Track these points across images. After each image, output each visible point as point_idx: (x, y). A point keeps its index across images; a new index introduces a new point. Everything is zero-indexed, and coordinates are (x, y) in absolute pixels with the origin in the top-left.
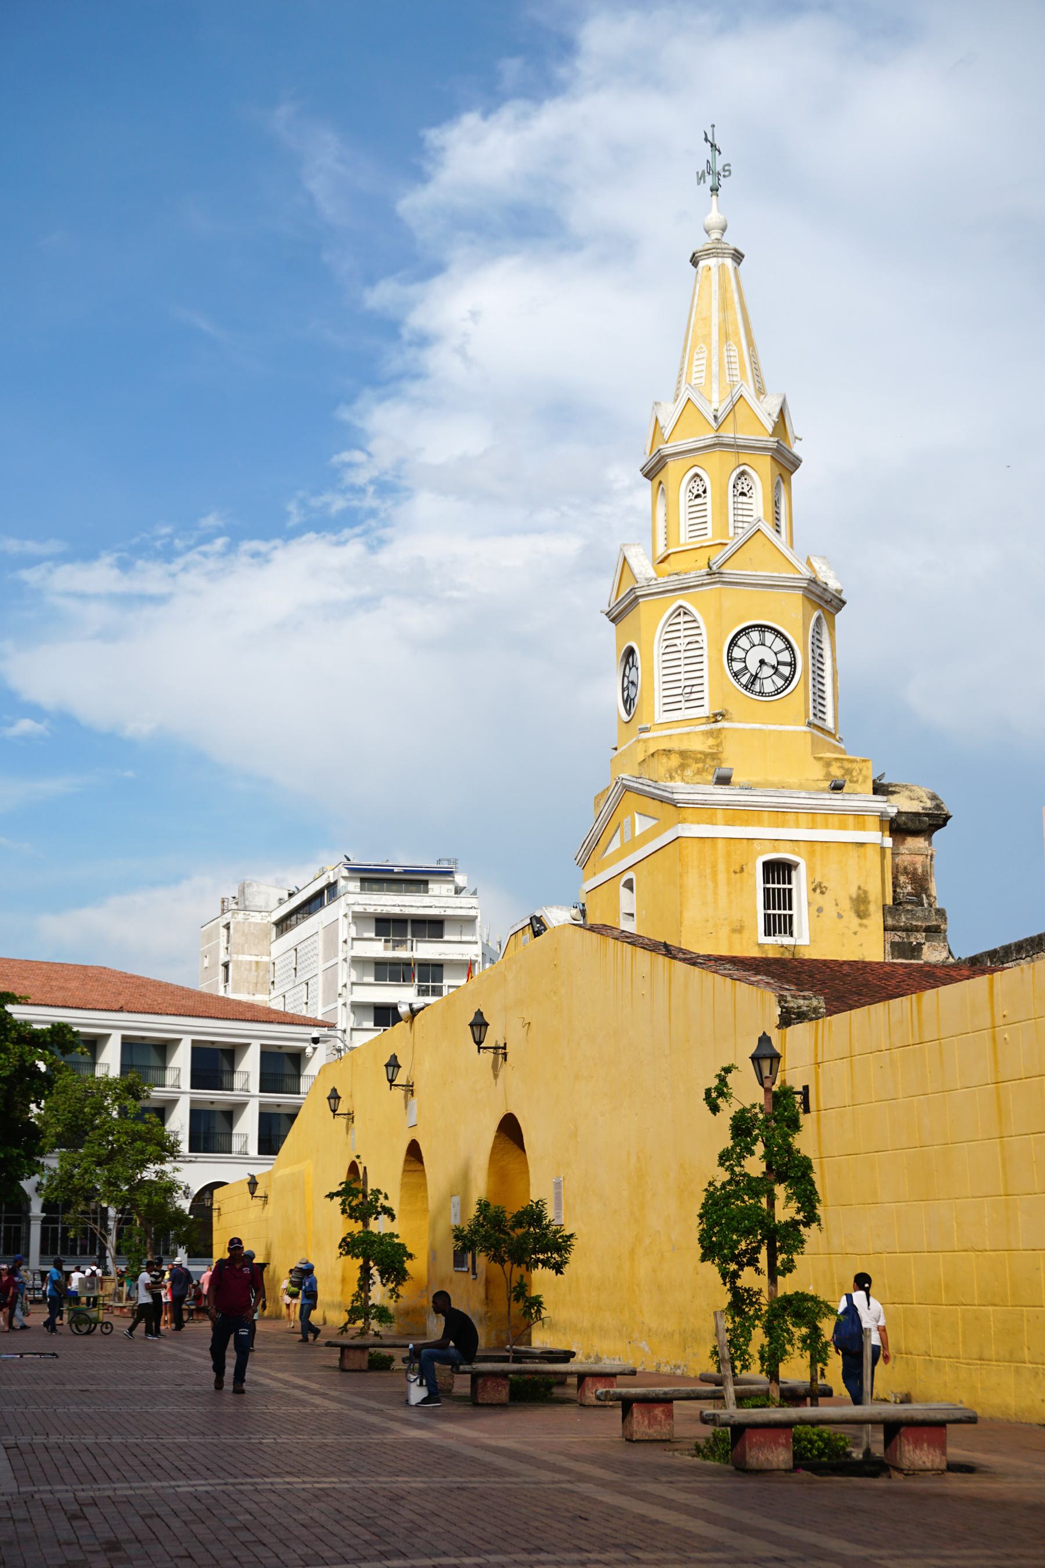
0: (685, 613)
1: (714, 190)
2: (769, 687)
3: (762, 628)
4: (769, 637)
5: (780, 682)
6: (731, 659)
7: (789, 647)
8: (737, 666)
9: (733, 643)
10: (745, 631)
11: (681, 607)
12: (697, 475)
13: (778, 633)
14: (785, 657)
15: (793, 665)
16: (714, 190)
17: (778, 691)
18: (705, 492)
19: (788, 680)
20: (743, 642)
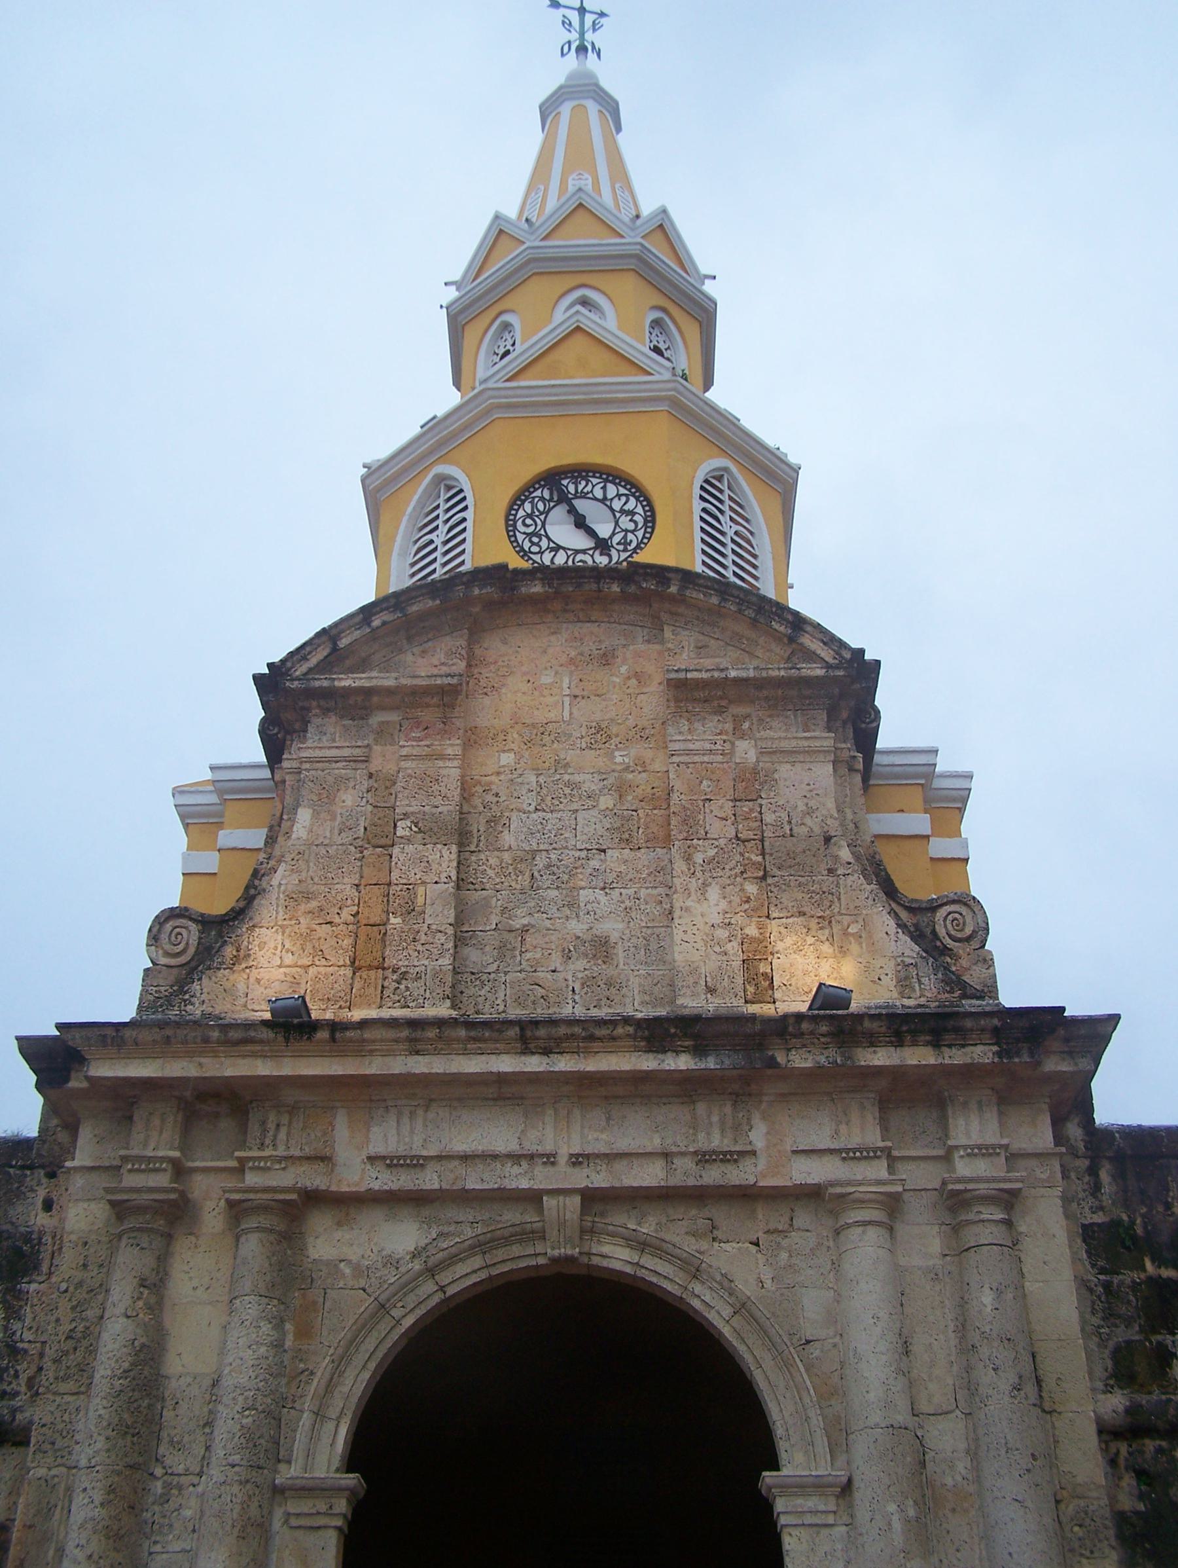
0: (449, 488)
11: (441, 479)
12: (507, 326)
13: (611, 475)
18: (513, 345)
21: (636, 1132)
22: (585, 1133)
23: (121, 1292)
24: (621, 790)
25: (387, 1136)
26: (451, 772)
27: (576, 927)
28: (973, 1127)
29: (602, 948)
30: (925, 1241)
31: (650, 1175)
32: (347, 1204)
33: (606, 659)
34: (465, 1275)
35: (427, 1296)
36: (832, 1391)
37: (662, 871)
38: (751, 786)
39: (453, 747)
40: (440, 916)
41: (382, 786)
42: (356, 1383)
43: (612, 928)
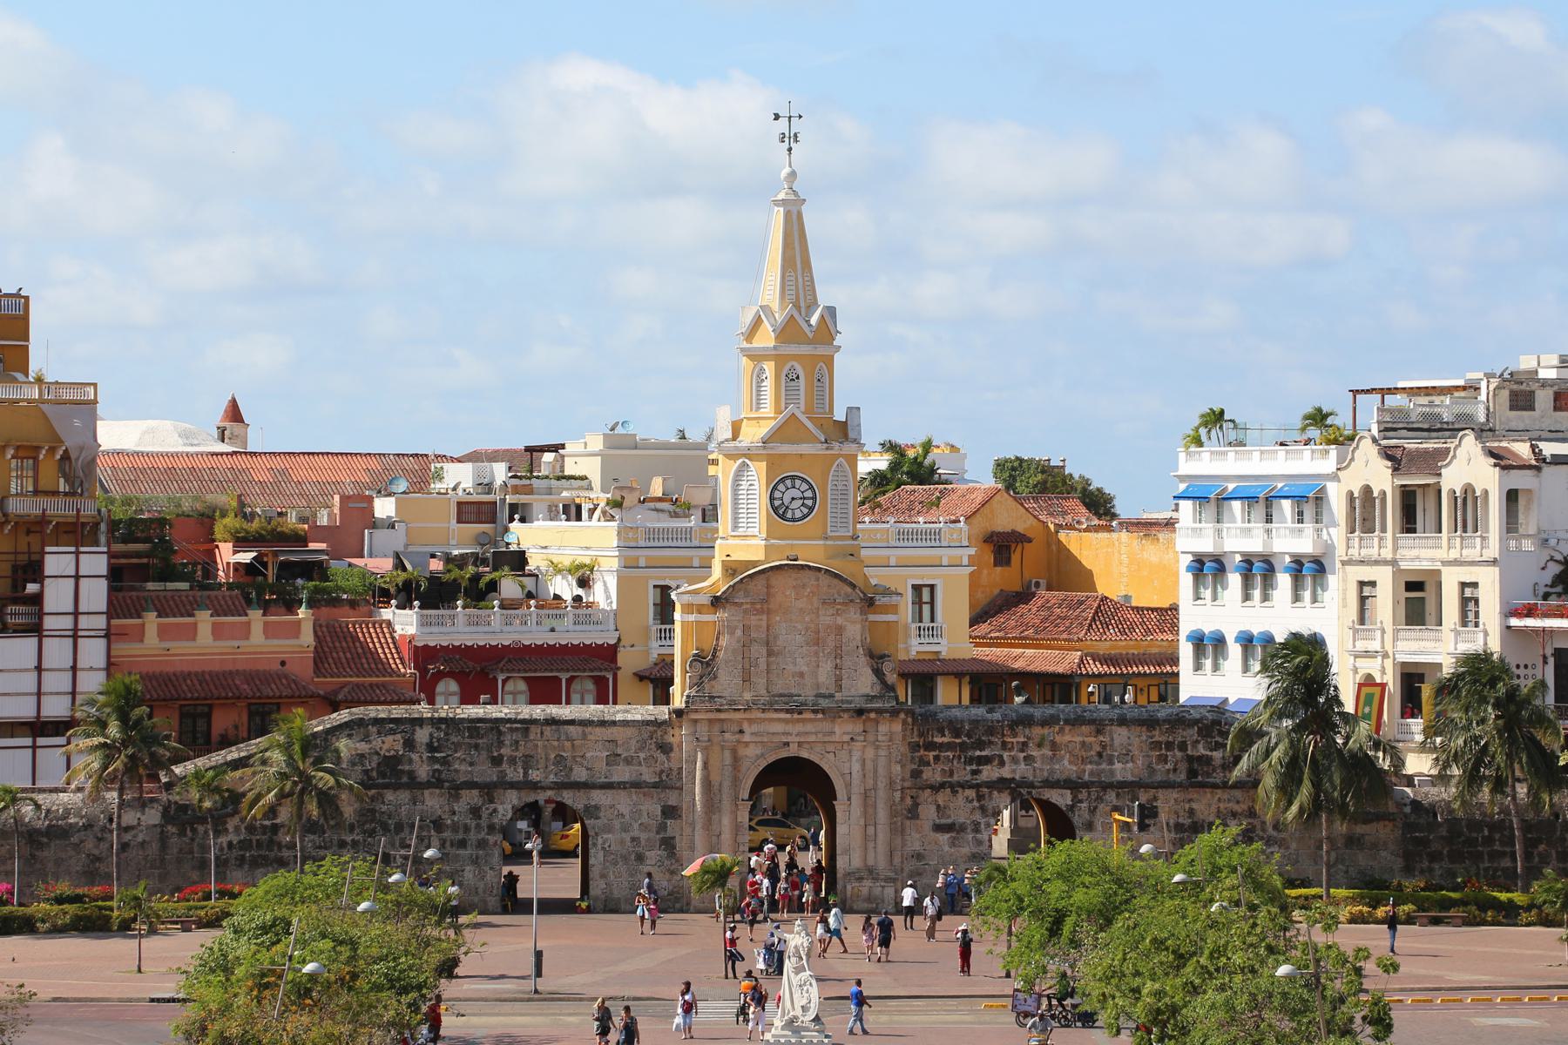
1: (790, 150)
2: (798, 514)
3: (793, 478)
4: (798, 482)
5: (806, 511)
6: (772, 499)
7: (811, 487)
8: (777, 503)
9: (775, 488)
10: (782, 480)
13: (803, 480)
14: (809, 494)
15: (814, 498)
16: (790, 150)
17: (805, 517)
19: (811, 509)
20: (781, 487)
21: (809, 727)
22: (799, 728)
23: (699, 764)
24: (807, 629)
25: (755, 728)
26: (764, 624)
27: (797, 669)
28: (883, 728)
29: (802, 675)
30: (870, 753)
31: (812, 738)
32: (747, 744)
33: (804, 586)
34: (771, 759)
35: (764, 764)
36: (848, 785)
37: (816, 653)
38: (840, 630)
39: (764, 617)
40: (763, 666)
41: (746, 629)
42: (750, 782)
43: (804, 669)
